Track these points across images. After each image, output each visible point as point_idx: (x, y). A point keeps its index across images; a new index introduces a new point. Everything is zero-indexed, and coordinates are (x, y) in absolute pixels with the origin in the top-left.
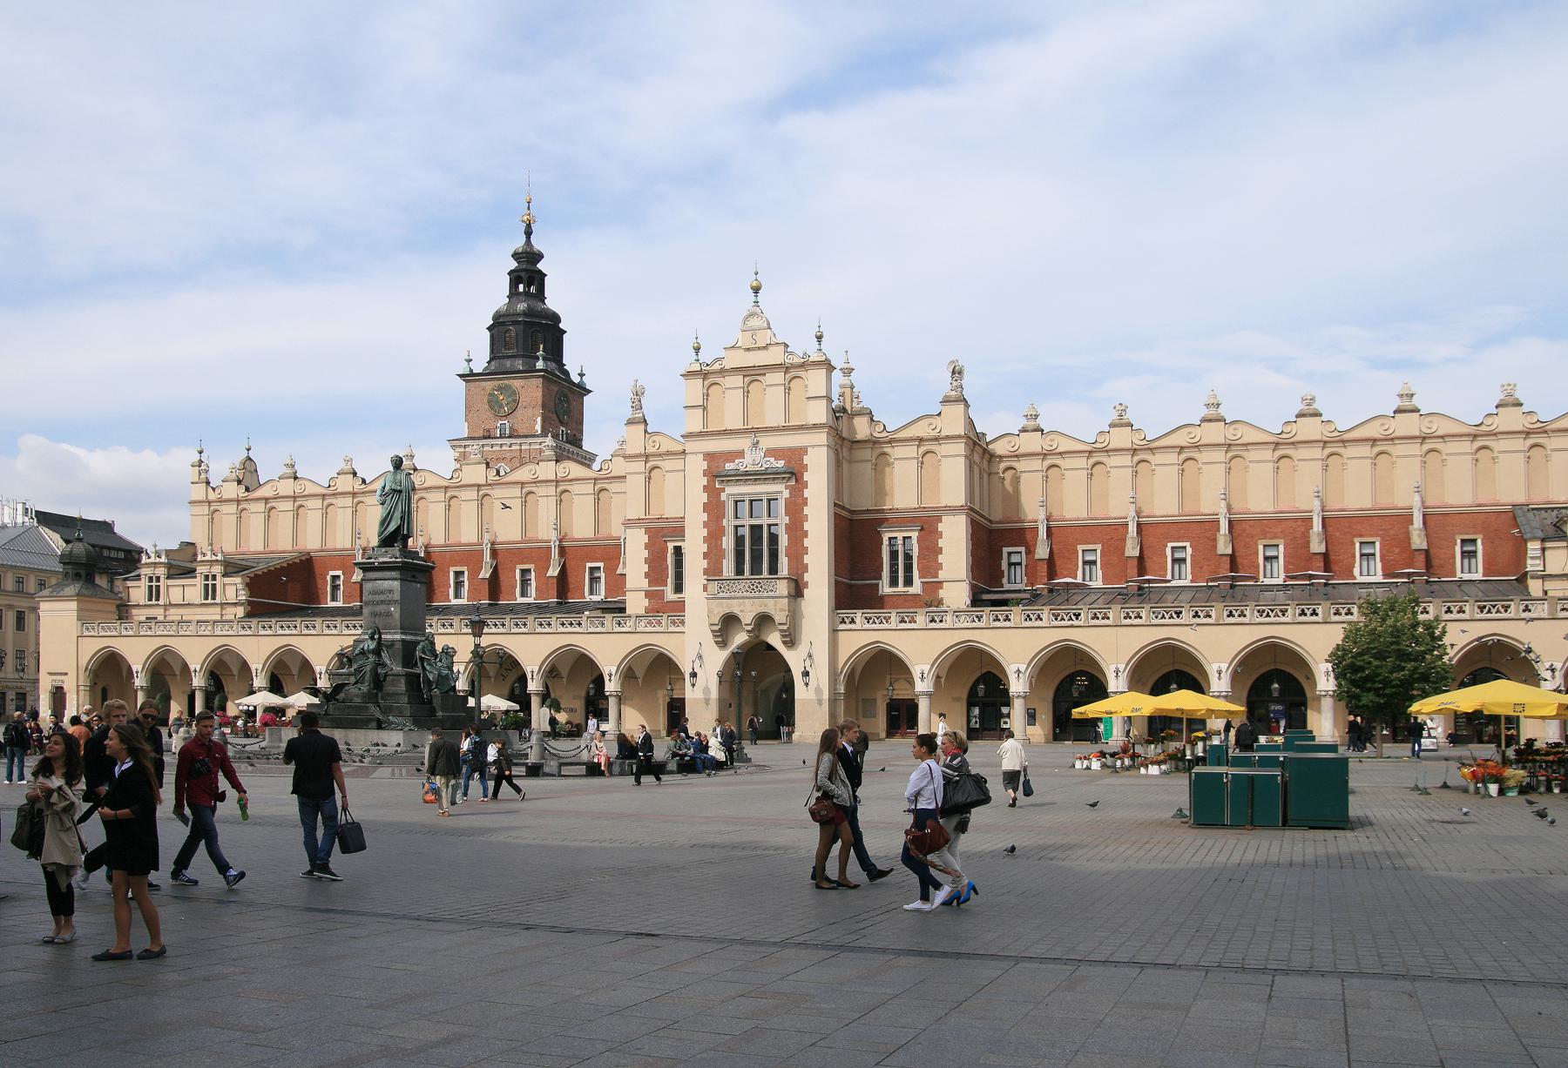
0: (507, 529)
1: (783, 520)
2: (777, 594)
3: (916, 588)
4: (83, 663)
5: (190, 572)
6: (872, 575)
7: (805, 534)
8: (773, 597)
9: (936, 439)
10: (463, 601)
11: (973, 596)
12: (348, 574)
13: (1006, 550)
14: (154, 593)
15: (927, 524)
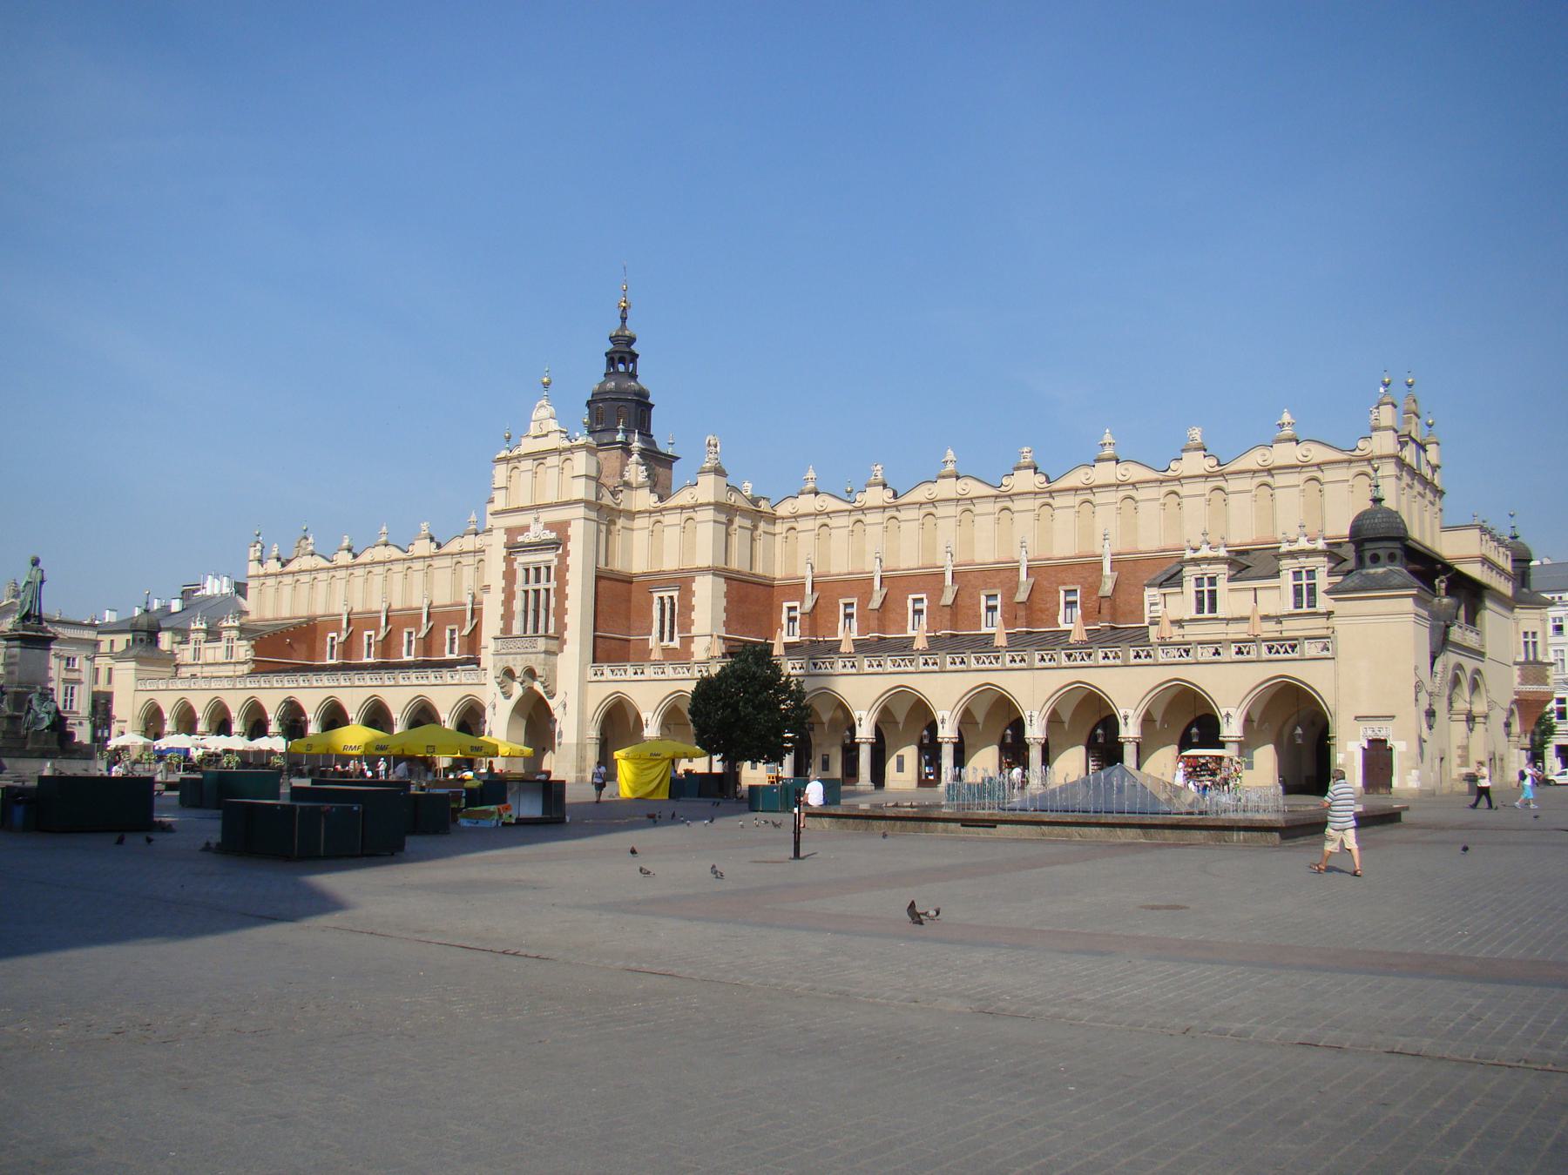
0: (442, 597)
1: (553, 585)
2: (538, 650)
3: (676, 643)
4: (137, 713)
5: (219, 639)
6: (646, 631)
7: (566, 597)
8: (536, 653)
9: (693, 507)
10: (411, 658)
11: (727, 649)
12: (339, 636)
13: (786, 605)
14: (197, 651)
15: (683, 581)
